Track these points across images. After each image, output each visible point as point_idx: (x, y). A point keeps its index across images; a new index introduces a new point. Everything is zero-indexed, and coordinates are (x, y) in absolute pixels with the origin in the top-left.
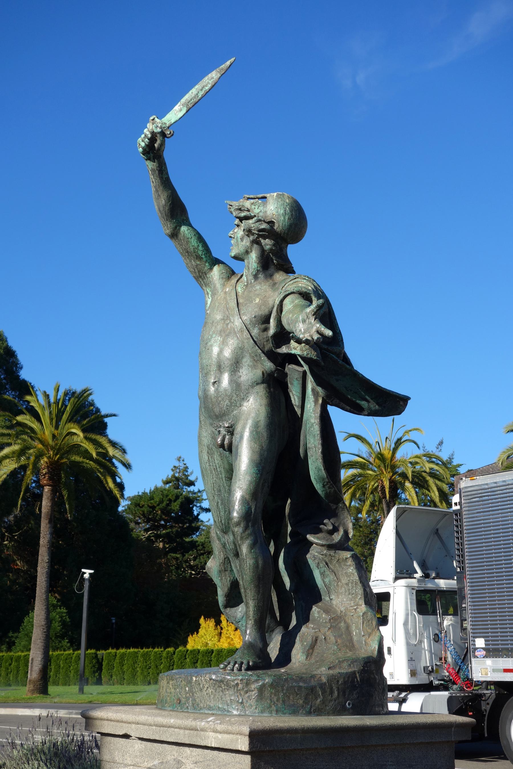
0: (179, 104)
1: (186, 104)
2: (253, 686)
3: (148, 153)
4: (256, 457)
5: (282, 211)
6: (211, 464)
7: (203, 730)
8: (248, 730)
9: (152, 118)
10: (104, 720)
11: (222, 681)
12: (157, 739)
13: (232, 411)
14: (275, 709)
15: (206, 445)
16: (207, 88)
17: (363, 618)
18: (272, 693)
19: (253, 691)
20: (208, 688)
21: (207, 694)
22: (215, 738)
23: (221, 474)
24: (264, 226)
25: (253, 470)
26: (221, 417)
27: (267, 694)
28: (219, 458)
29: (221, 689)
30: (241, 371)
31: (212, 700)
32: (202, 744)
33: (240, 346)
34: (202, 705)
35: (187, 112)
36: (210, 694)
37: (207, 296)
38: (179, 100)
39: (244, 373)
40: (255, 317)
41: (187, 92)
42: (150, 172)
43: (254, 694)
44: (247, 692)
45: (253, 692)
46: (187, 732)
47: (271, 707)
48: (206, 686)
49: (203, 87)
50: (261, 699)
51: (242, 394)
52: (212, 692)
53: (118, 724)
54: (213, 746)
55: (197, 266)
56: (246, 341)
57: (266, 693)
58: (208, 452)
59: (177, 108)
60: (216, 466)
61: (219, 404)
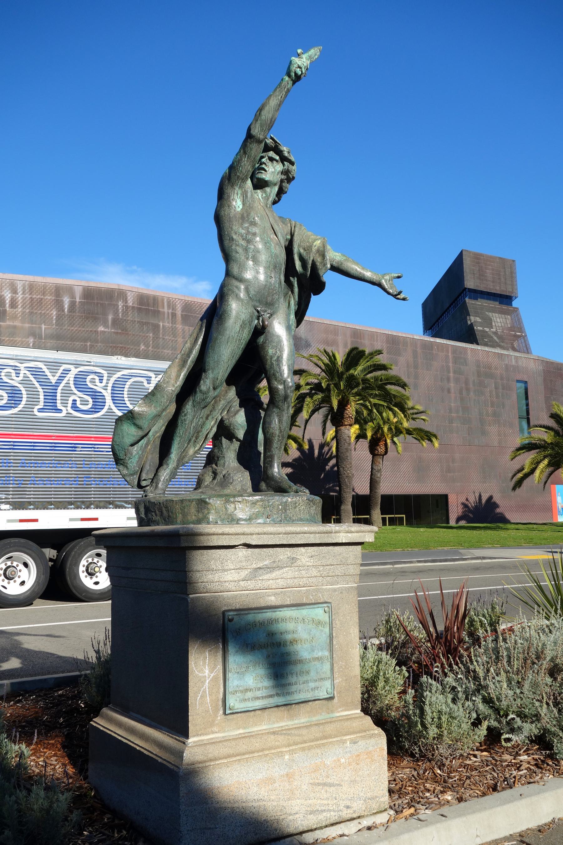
7: (336, 532)
10: (214, 534)
12: (285, 543)
15: (242, 319)
22: (345, 537)
26: (270, 305)
28: (247, 333)
32: (333, 542)
34: (294, 518)
42: (286, 89)
46: (317, 535)
53: (233, 537)
54: (344, 542)
55: (249, 171)
58: (241, 326)
61: (273, 295)
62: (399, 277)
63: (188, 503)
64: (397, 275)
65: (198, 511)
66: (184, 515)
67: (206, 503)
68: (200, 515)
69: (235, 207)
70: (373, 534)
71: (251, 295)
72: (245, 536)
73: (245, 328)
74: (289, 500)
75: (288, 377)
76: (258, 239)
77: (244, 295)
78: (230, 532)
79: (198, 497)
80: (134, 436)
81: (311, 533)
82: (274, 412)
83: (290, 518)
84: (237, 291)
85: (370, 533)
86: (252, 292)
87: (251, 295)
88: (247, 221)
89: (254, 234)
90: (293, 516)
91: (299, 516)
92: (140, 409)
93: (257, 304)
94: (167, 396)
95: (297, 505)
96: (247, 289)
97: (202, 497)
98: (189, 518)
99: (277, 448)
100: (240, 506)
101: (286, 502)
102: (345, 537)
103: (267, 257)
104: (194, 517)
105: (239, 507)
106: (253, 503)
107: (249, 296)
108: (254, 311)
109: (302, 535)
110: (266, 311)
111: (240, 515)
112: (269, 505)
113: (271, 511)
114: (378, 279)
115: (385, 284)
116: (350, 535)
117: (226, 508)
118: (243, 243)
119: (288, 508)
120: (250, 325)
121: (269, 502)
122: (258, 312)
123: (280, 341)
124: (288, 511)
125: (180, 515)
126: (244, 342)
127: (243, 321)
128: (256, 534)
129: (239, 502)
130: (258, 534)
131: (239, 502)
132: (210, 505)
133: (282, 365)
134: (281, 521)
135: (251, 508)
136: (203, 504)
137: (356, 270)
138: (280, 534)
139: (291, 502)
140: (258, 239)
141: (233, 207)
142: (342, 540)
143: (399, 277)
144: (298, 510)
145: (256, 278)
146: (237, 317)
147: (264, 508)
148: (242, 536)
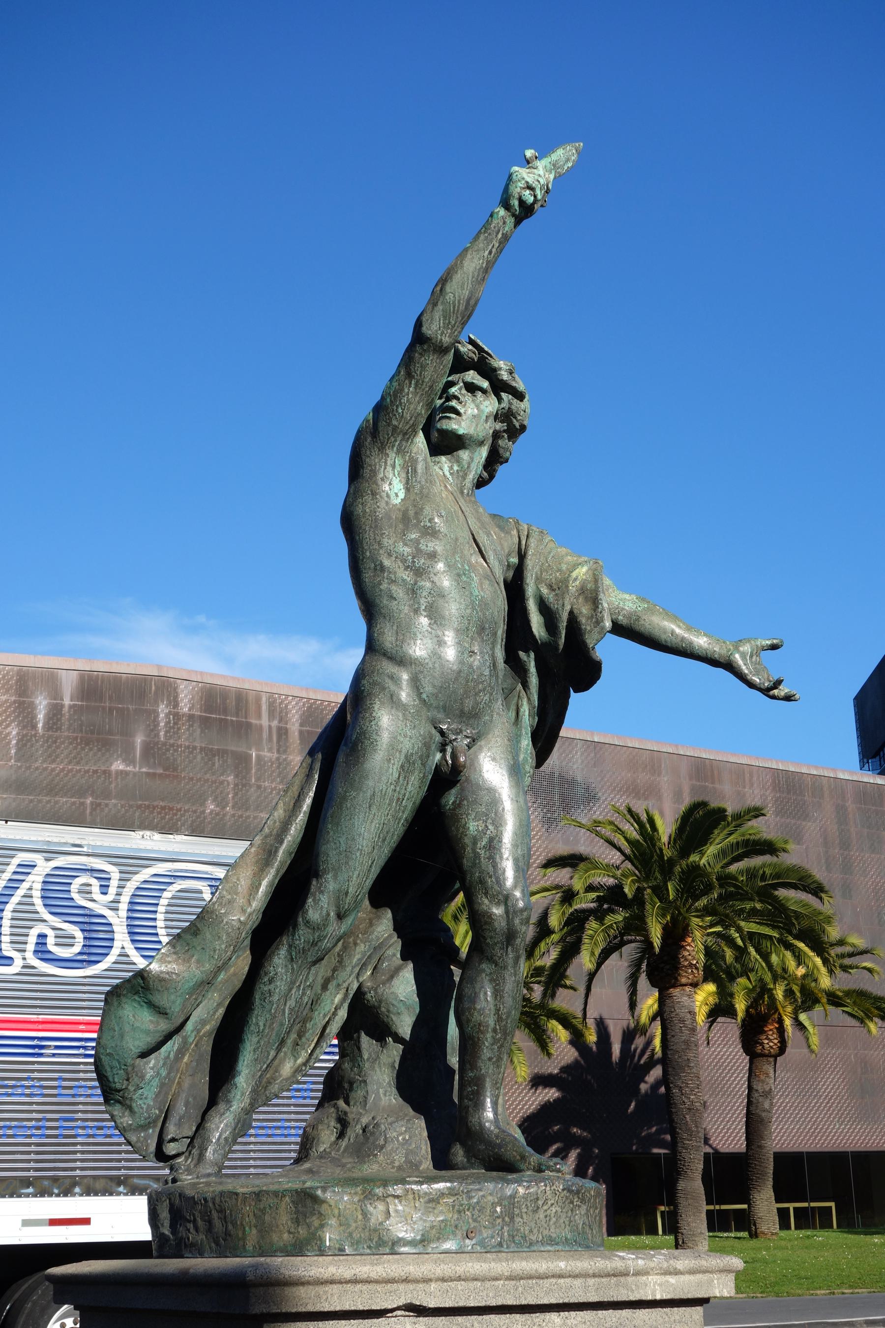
6: (398, 789)
7: (637, 1273)
10: (332, 1282)
12: (510, 1302)
15: (404, 751)
20: (552, 1205)
21: (546, 1217)
22: (660, 1285)
23: (403, 812)
26: (469, 718)
28: (417, 783)
31: (553, 1227)
32: (632, 1298)
34: (534, 1238)
36: (552, 1215)
37: (389, 468)
42: (500, 236)
46: (591, 1281)
48: (550, 1203)
52: (556, 1211)
53: (379, 1287)
54: (658, 1297)
55: (419, 415)
58: (402, 766)
60: (404, 795)
61: (476, 694)
62: (774, 647)
63: (272, 1201)
64: (769, 642)
65: (297, 1222)
66: (264, 1230)
67: (315, 1199)
68: (302, 1232)
69: (388, 496)
70: (732, 1277)
71: (424, 696)
72: (411, 1286)
73: (412, 772)
74: (521, 1190)
75: (515, 886)
76: (440, 566)
77: (408, 695)
78: (373, 1276)
79: (297, 1186)
80: (147, 1032)
81: (576, 1276)
82: (484, 971)
83: (524, 1237)
84: (393, 687)
85: (723, 1276)
86: (428, 689)
87: (424, 696)
88: (416, 526)
89: (433, 556)
90: (531, 1231)
91: (546, 1232)
92: (163, 968)
93: (440, 716)
94: (228, 934)
95: (540, 1203)
96: (415, 682)
97: (308, 1184)
98: (275, 1237)
99: (490, 1059)
100: (400, 1208)
101: (513, 1196)
102: (660, 1285)
103: (463, 607)
104: (286, 1236)
105: (396, 1211)
106: (431, 1201)
108: (434, 731)
109: (554, 1280)
110: (461, 731)
111: (402, 1231)
112: (469, 1205)
113: (475, 1220)
114: (724, 652)
115: (741, 662)
116: (672, 1280)
117: (365, 1214)
118: (407, 576)
119: (517, 1211)
120: (423, 765)
121: (470, 1198)
122: (442, 733)
123: (495, 802)
124: (518, 1219)
125: (254, 1231)
127: (406, 757)
129: (397, 1197)
130: (443, 1280)
131: (397, 1197)
132: (324, 1206)
133: (501, 858)
134: (500, 1244)
135: (427, 1212)
136: (309, 1202)
137: (673, 632)
138: (497, 1279)
139: (525, 1197)
140: (440, 566)
141: (384, 495)
142: (653, 1293)
143: (774, 647)
144: (542, 1216)
145: (436, 655)
146: (393, 747)
147: (459, 1212)
148: (402, 1287)
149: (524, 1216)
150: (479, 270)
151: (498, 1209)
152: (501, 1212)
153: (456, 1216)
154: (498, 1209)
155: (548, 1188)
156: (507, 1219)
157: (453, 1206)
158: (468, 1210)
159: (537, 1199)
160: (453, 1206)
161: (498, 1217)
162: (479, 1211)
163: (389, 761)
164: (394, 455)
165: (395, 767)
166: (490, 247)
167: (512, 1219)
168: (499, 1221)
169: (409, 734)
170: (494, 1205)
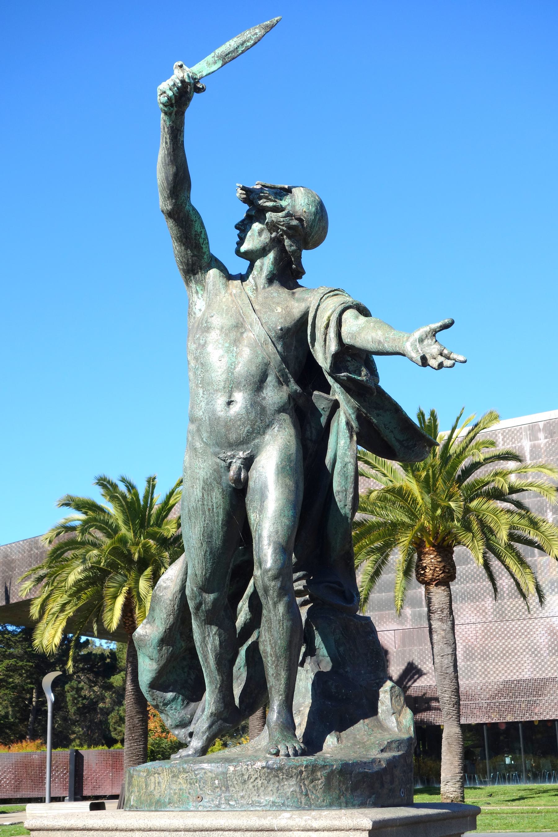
0: (213, 54)
1: (220, 57)
2: (319, 774)
3: (172, 105)
4: (292, 498)
5: (314, 209)
6: (205, 503)
8: (371, 823)
9: (180, 63)
11: (280, 769)
13: (254, 439)
14: (344, 800)
15: (201, 478)
16: (249, 44)
17: (391, 694)
18: (340, 781)
19: (319, 779)
20: (256, 778)
21: (254, 787)
23: (218, 516)
24: (295, 222)
25: (291, 513)
27: (335, 782)
29: (277, 779)
30: (264, 391)
31: (262, 794)
33: (265, 361)
35: (222, 66)
36: (260, 786)
37: (195, 295)
38: (213, 50)
39: (269, 394)
40: (281, 329)
41: (223, 43)
43: (320, 783)
44: (312, 781)
45: (320, 781)
47: (339, 798)
48: (254, 777)
49: (244, 42)
50: (329, 789)
51: (267, 421)
52: (262, 783)
56: (272, 356)
57: (334, 781)
58: (203, 488)
59: (210, 58)
60: (213, 505)
64: (439, 324)
70: (368, 832)
71: (204, 440)
80: (152, 670)
93: (217, 449)
94: (165, 608)
107: (203, 441)
108: (218, 460)
109: (221, 833)
113: (201, 790)
119: (230, 783)
120: (220, 483)
121: (196, 775)
124: (231, 789)
126: (221, 511)
127: (204, 481)
128: (140, 830)
134: (218, 806)
144: (251, 786)
147: (191, 784)
149: (236, 786)
150: (164, 157)
151: (217, 782)
152: (219, 784)
153: (189, 786)
154: (217, 782)
155: (250, 767)
156: (223, 788)
157: (187, 780)
158: (196, 782)
159: (243, 775)
160: (187, 780)
161: (217, 787)
162: (204, 783)
163: (193, 487)
164: (195, 286)
165: (198, 490)
166: (164, 140)
167: (227, 788)
168: (218, 789)
169: (202, 466)
170: (213, 779)
